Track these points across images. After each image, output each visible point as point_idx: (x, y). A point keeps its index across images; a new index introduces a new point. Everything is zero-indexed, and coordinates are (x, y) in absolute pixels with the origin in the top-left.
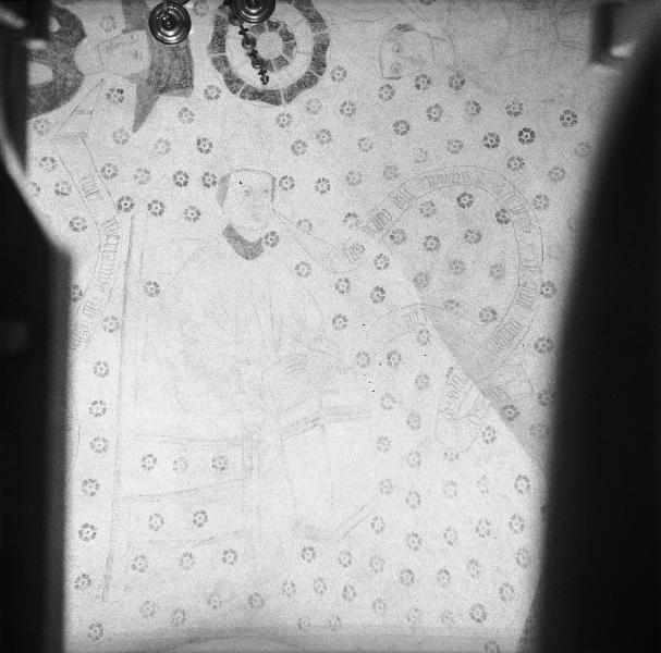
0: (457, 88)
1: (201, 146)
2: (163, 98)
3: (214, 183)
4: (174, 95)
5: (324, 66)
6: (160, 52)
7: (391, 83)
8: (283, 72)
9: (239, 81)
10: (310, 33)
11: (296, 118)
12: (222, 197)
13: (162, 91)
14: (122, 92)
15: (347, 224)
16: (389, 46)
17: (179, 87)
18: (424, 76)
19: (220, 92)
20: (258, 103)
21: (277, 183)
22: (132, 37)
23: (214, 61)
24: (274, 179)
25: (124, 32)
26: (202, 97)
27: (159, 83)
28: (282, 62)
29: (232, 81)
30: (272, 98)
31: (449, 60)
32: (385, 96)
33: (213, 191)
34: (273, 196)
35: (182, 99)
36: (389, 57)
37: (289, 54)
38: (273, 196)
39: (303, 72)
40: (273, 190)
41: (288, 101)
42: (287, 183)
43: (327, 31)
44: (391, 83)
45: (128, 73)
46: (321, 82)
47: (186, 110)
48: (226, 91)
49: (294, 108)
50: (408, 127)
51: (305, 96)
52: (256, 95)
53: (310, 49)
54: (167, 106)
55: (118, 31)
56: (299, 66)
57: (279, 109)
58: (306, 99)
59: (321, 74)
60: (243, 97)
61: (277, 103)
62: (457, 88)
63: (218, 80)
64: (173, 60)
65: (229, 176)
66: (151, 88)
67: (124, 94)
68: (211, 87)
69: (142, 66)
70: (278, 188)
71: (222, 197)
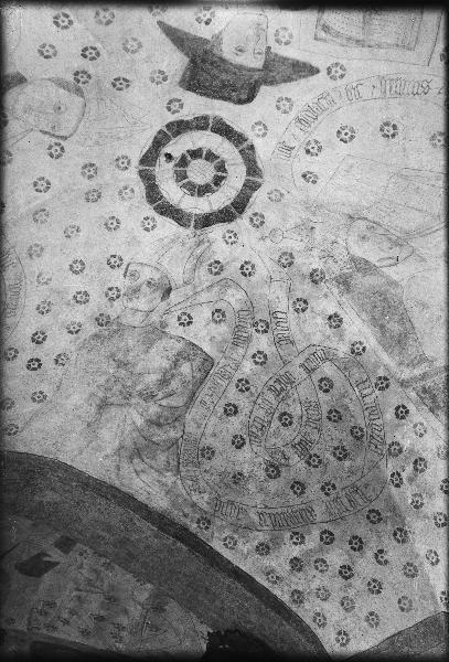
0: (97, 319)
1: (121, 81)
2: (187, 60)
3: (78, 81)
4: (185, 73)
6: (235, 73)
7: (124, 267)
8: (172, 172)
9: (178, 133)
10: (198, 212)
12: (61, 84)
13: (193, 61)
14: (207, 23)
16: (157, 276)
17: (193, 77)
19: (173, 113)
20: (150, 143)
21: (60, 141)
22: (259, 53)
23: (205, 118)
24: (65, 138)
25: (269, 48)
26: (174, 96)
27: (203, 61)
28: (181, 176)
29: (179, 128)
30: (149, 159)
33: (70, 78)
34: (46, 133)
35: (178, 78)
37: (184, 186)
38: (46, 133)
40: (53, 135)
41: (141, 173)
42: (57, 152)
45: (224, 34)
47: (165, 79)
48: (172, 118)
49: (132, 176)
50: (76, 272)
51: (140, 189)
52: (159, 142)
53: (182, 206)
54: (175, 62)
55: (271, 43)
56: (172, 192)
57: (135, 161)
60: (159, 132)
61: (142, 162)
62: (97, 319)
63: (186, 114)
64: (222, 81)
65: (82, 96)
66: (200, 52)
67: (203, 24)
68: (181, 106)
69: (227, 52)
70: (54, 140)
71: (61, 84)
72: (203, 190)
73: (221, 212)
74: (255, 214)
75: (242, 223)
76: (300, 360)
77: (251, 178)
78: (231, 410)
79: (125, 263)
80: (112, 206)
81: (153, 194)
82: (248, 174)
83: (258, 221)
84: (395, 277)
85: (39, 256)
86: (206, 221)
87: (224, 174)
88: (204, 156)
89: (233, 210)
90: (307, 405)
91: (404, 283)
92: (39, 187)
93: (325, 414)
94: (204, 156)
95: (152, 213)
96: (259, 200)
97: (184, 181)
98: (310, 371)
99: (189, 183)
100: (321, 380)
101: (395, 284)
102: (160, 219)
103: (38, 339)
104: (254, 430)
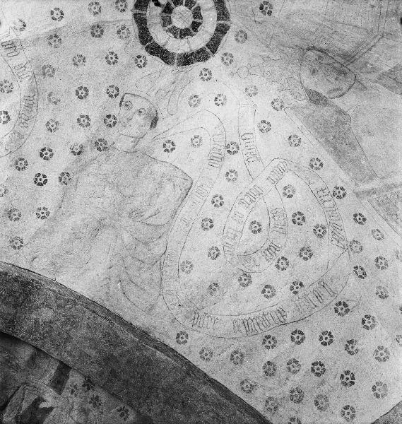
0: (96, 144)
5: (151, 53)
7: (119, 98)
10: (179, 52)
11: (120, 16)
15: (17, 21)
18: (115, 123)
28: (166, 22)
31: (118, 145)
32: (111, 90)
36: (137, 104)
37: (170, 30)
39: (153, 35)
41: (135, 15)
43: (175, 65)
44: (119, 98)
46: (140, 46)
50: (81, 98)
51: (134, 29)
53: (168, 47)
56: (160, 36)
58: (131, 29)
59: (147, 48)
61: (136, 6)
62: (96, 144)
72: (184, 33)
73: (198, 52)
74: (225, 54)
75: (214, 62)
76: (266, 174)
77: (222, 22)
78: (208, 224)
79: (121, 94)
80: (111, 42)
81: (145, 37)
82: (219, 19)
83: (228, 59)
84: (342, 107)
85: (51, 76)
86: (187, 60)
87: (200, 21)
88: (184, 3)
89: (208, 50)
90: (273, 213)
91: (351, 112)
92: (55, 15)
93: (290, 218)
94: (184, 3)
95: (144, 53)
96: (229, 41)
97: (170, 26)
98: (275, 182)
99: (174, 27)
100: (285, 188)
101: (340, 112)
102: (149, 57)
103: (45, 154)
104: (227, 240)
